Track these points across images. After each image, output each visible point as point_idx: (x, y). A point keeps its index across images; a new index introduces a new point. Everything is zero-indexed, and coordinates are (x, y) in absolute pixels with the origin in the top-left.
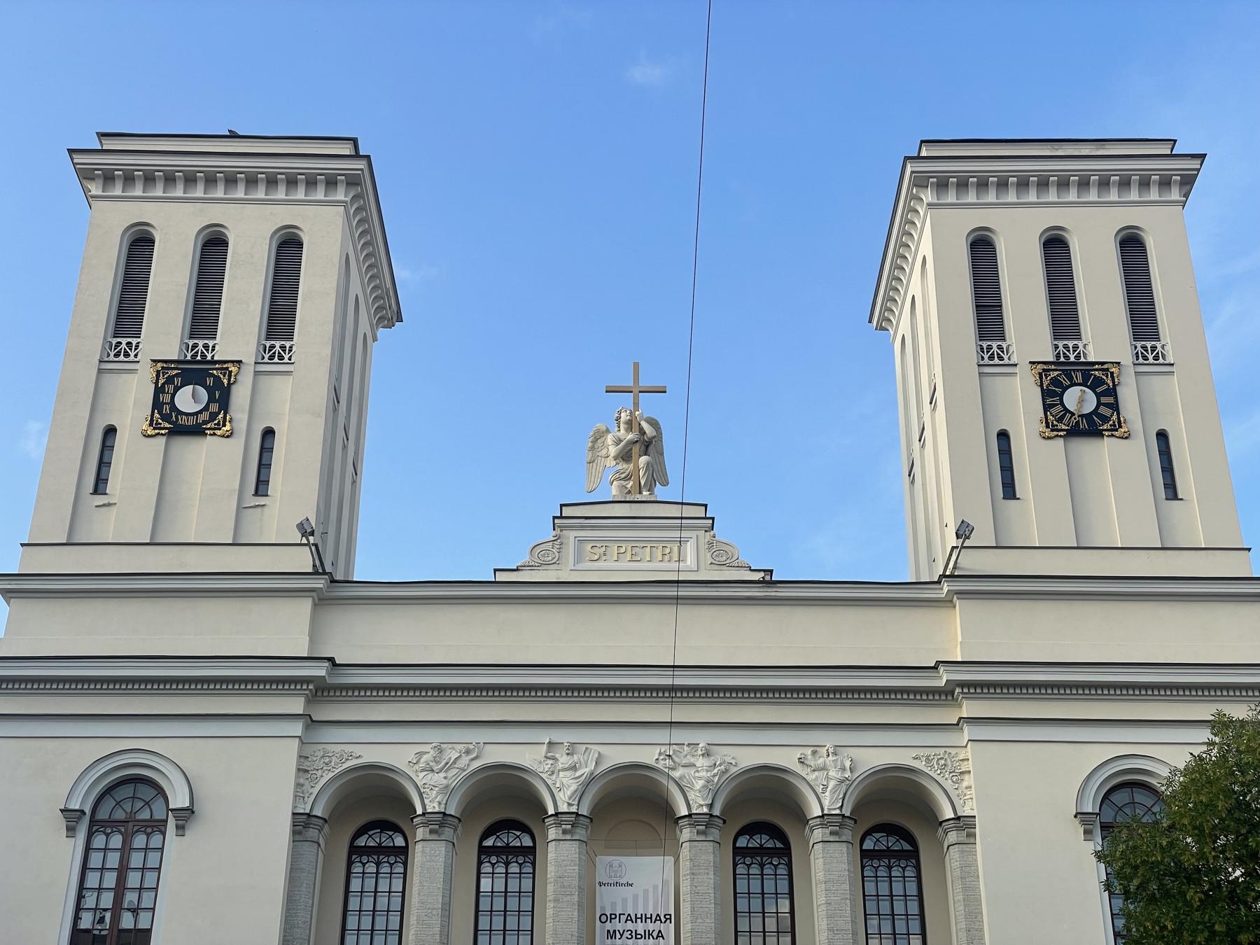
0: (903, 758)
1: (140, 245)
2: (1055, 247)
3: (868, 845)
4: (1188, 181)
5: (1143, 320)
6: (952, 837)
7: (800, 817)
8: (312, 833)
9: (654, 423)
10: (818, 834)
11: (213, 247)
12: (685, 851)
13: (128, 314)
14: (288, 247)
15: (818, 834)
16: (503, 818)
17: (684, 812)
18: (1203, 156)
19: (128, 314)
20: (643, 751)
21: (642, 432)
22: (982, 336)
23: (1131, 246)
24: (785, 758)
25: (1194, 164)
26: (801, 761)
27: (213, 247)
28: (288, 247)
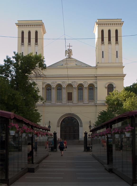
0: (92, 82)
1: (23, 33)
2: (109, 31)
3: (89, 88)
4: (122, 24)
5: (117, 40)
6: (96, 89)
7: (84, 86)
8: (44, 89)
9: (71, 50)
10: (85, 89)
11: (29, 33)
12: (74, 90)
13: (23, 41)
14: (36, 32)
15: (85, 89)
16: (59, 87)
17: (74, 87)
18: (124, 22)
19: (23, 41)
20: (70, 82)
21: (70, 51)
22: (102, 41)
23: (117, 31)
24: (82, 82)
25: (123, 22)
26: (83, 82)
27: (29, 33)
28: (36, 32)
